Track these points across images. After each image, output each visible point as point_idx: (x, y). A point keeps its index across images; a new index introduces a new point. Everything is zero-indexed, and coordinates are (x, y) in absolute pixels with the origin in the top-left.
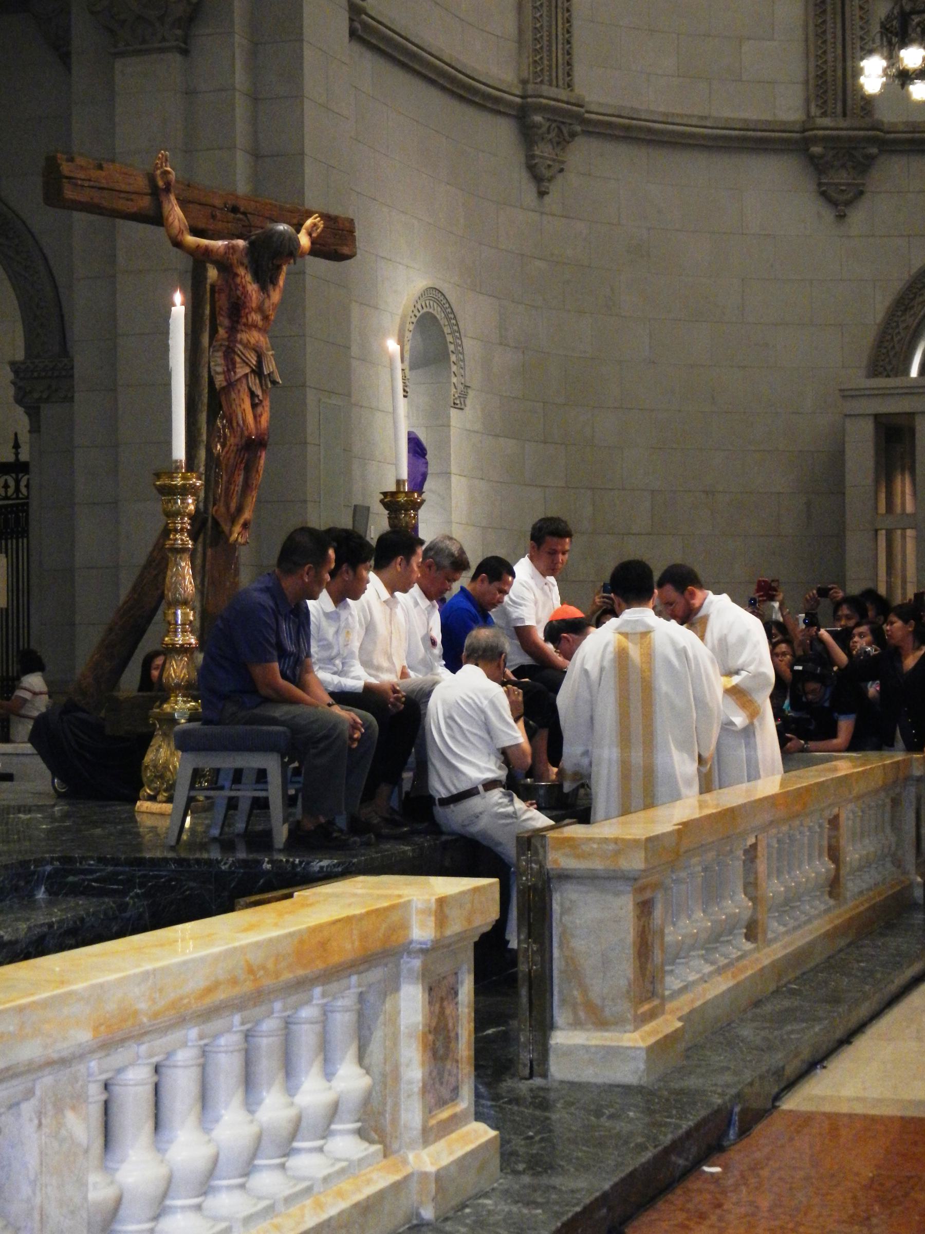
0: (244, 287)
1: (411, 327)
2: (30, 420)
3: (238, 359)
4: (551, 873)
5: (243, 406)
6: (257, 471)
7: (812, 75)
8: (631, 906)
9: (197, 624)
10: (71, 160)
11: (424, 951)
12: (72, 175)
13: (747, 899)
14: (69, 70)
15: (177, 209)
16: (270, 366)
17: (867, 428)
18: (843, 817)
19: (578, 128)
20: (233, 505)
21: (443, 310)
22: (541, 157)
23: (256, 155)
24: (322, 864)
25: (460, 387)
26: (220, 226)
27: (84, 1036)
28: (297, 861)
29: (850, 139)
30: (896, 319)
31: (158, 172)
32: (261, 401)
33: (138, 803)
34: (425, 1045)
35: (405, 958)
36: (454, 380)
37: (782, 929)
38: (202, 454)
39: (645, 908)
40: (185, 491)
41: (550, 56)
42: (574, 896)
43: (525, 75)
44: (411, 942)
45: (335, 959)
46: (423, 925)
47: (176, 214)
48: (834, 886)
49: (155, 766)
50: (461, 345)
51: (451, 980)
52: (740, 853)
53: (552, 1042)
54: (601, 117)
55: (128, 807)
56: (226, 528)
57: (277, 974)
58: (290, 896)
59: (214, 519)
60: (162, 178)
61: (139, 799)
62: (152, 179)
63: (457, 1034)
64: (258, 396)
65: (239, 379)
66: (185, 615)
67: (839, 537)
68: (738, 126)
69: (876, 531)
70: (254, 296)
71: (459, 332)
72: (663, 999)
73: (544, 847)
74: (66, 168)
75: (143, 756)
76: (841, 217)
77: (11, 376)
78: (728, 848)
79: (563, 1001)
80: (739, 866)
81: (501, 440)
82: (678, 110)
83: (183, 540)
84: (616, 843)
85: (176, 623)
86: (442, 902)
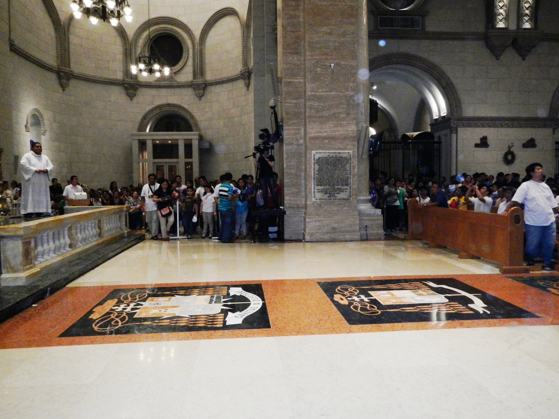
1: (30, 117)
17: (137, 141)
19: (72, 77)
25: (44, 131)
29: (132, 84)
36: (42, 129)
37: (81, 245)
39: (27, 244)
42: (5, 241)
43: (59, 64)
48: (100, 235)
69: (139, 163)
76: (131, 99)
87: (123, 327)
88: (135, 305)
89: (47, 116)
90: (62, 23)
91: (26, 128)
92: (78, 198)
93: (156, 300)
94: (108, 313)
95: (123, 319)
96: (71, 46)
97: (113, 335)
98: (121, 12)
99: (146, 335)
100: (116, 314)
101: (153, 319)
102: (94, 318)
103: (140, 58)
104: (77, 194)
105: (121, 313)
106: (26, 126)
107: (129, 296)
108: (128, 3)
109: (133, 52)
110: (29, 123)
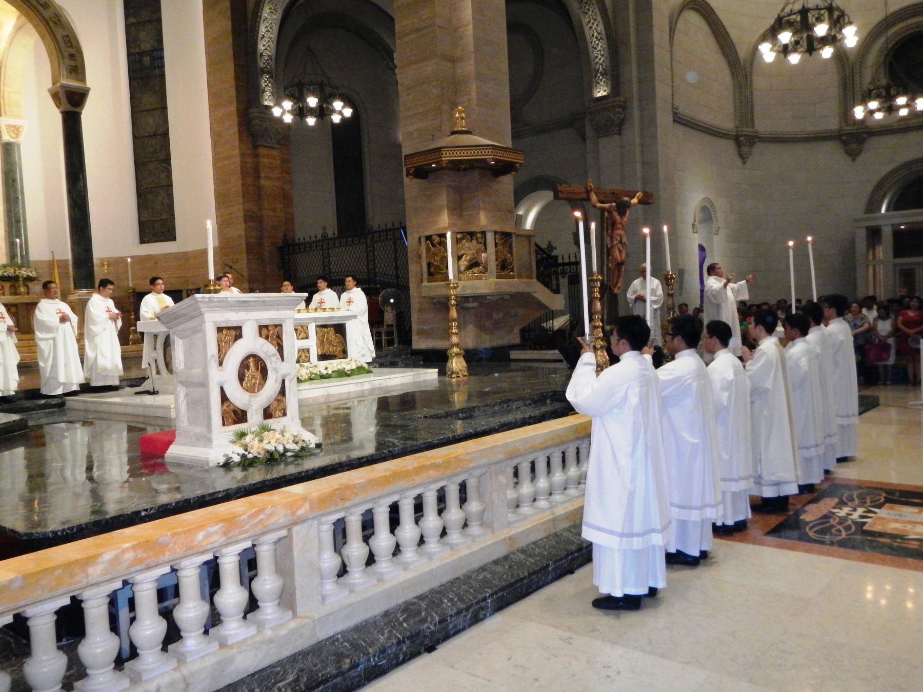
9: (605, 317)
16: (624, 240)
19: (756, 140)
20: (615, 282)
23: (643, 163)
26: (608, 199)
27: (501, 456)
38: (605, 267)
40: (597, 280)
47: (594, 198)
62: (586, 188)
67: (854, 269)
69: (867, 266)
76: (854, 160)
87: (849, 539)
88: (864, 512)
89: (721, 205)
90: (742, 62)
93: (897, 508)
94: (826, 517)
95: (848, 528)
96: (755, 92)
97: (835, 548)
98: (837, 35)
99: (882, 556)
100: (837, 520)
101: (893, 537)
102: (808, 519)
103: (870, 91)
105: (842, 520)
106: (693, 225)
107: (855, 496)
108: (849, 19)
109: (857, 78)
110: (697, 221)
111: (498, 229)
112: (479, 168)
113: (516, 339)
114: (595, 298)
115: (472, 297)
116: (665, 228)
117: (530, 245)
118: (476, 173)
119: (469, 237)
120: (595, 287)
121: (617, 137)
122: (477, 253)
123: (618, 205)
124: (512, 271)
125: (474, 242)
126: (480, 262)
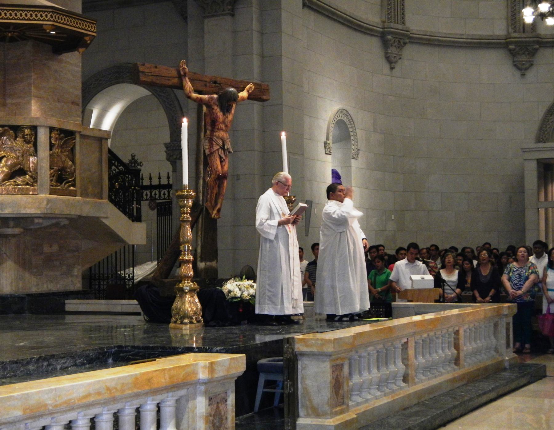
0: (216, 114)
1: (333, 125)
2: (173, 166)
3: (214, 143)
4: (297, 353)
5: (217, 162)
6: (223, 188)
7: (510, 15)
8: (329, 366)
9: (199, 250)
10: (143, 65)
11: (205, 383)
12: (144, 71)
13: (403, 365)
14: (186, 22)
15: (189, 84)
16: (228, 145)
17: (533, 165)
18: (461, 332)
19: (407, 41)
21: (348, 118)
22: (392, 53)
23: (262, 56)
24: (217, 349)
26: (208, 89)
27: (18, 413)
28: (208, 347)
29: (526, 42)
30: (548, 118)
31: (181, 68)
32: (224, 160)
33: (170, 324)
34: (207, 421)
35: (198, 386)
36: (353, 147)
37: (424, 378)
38: (201, 182)
39: (337, 368)
40: (187, 197)
41: (395, 10)
42: (306, 362)
43: (384, 19)
44: (199, 380)
45: (156, 386)
46: (204, 372)
48: (457, 361)
49: (176, 309)
50: (356, 133)
51: (223, 395)
52: (400, 346)
53: (298, 423)
54: (418, 36)
55: (166, 326)
56: (210, 211)
57: (123, 391)
58: (155, 360)
59: (206, 208)
60: (183, 71)
61: (170, 323)
62: (179, 72)
63: (227, 418)
64: (223, 158)
65: (215, 150)
66: (188, 247)
67: (523, 212)
68: (478, 38)
69: (539, 209)
70: (221, 117)
71: (355, 127)
72: (348, 405)
73: (294, 342)
74: (141, 68)
75: (172, 305)
76: (523, 75)
77: (165, 149)
78: (391, 343)
79: (303, 406)
80: (399, 352)
81: (374, 172)
82: (449, 32)
83: (188, 217)
84: (322, 341)
85: (185, 251)
86: (212, 364)
91: (325, 147)
92: (416, 287)
104: (416, 277)
106: (325, 143)
110: (331, 138)
111: (54, 122)
112: (36, 39)
113: (78, 285)
114: (184, 221)
115: (14, 219)
116: (283, 136)
117: (101, 151)
118: (28, 46)
119: (12, 132)
120: (184, 206)
121: (228, 18)
122: (23, 156)
123: (220, 99)
124: (74, 186)
125: (20, 140)
126: (25, 169)
